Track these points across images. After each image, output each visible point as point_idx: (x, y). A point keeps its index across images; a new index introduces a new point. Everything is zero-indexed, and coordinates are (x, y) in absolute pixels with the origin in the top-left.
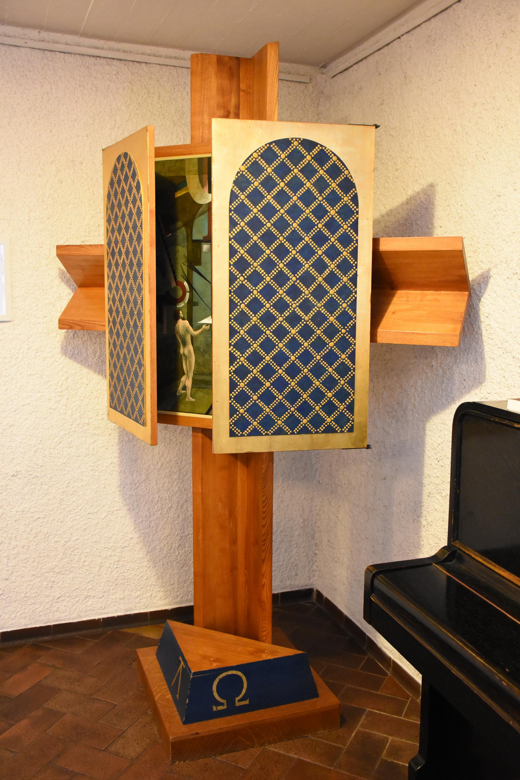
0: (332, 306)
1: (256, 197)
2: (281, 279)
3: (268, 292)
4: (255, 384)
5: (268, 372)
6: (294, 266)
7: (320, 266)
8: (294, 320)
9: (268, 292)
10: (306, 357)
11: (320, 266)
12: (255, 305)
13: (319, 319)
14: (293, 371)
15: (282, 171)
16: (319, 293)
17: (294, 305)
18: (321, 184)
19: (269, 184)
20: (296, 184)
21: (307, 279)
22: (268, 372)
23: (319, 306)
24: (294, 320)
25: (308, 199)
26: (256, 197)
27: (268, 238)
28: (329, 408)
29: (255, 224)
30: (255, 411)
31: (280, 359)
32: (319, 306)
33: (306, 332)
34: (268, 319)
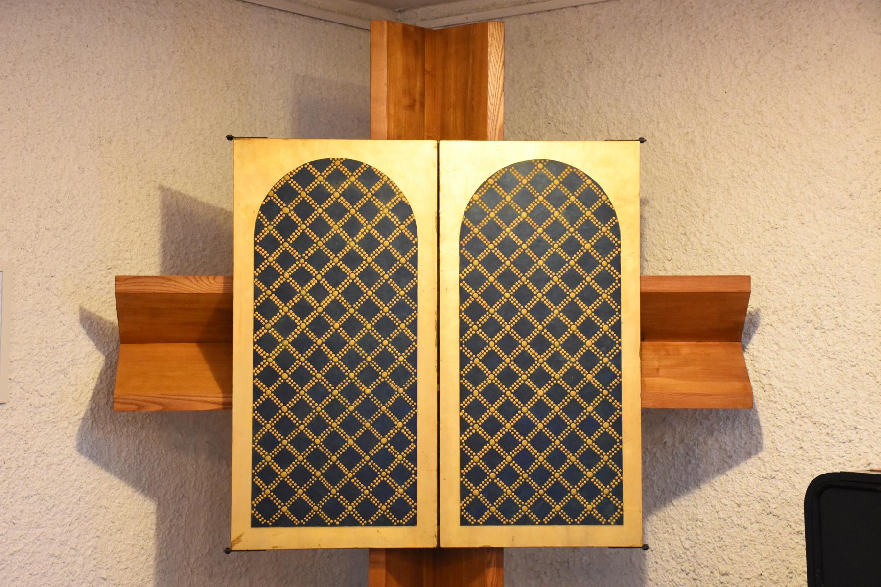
0: (589, 360)
3: (508, 344)
5: (508, 442)
7: (573, 312)
11: (573, 312)
13: (573, 377)
16: (573, 345)
17: (541, 360)
18: (573, 214)
22: (508, 442)
23: (573, 361)
28: (590, 492)
30: (492, 492)
31: (524, 426)
32: (573, 361)
33: (557, 394)
34: (508, 377)
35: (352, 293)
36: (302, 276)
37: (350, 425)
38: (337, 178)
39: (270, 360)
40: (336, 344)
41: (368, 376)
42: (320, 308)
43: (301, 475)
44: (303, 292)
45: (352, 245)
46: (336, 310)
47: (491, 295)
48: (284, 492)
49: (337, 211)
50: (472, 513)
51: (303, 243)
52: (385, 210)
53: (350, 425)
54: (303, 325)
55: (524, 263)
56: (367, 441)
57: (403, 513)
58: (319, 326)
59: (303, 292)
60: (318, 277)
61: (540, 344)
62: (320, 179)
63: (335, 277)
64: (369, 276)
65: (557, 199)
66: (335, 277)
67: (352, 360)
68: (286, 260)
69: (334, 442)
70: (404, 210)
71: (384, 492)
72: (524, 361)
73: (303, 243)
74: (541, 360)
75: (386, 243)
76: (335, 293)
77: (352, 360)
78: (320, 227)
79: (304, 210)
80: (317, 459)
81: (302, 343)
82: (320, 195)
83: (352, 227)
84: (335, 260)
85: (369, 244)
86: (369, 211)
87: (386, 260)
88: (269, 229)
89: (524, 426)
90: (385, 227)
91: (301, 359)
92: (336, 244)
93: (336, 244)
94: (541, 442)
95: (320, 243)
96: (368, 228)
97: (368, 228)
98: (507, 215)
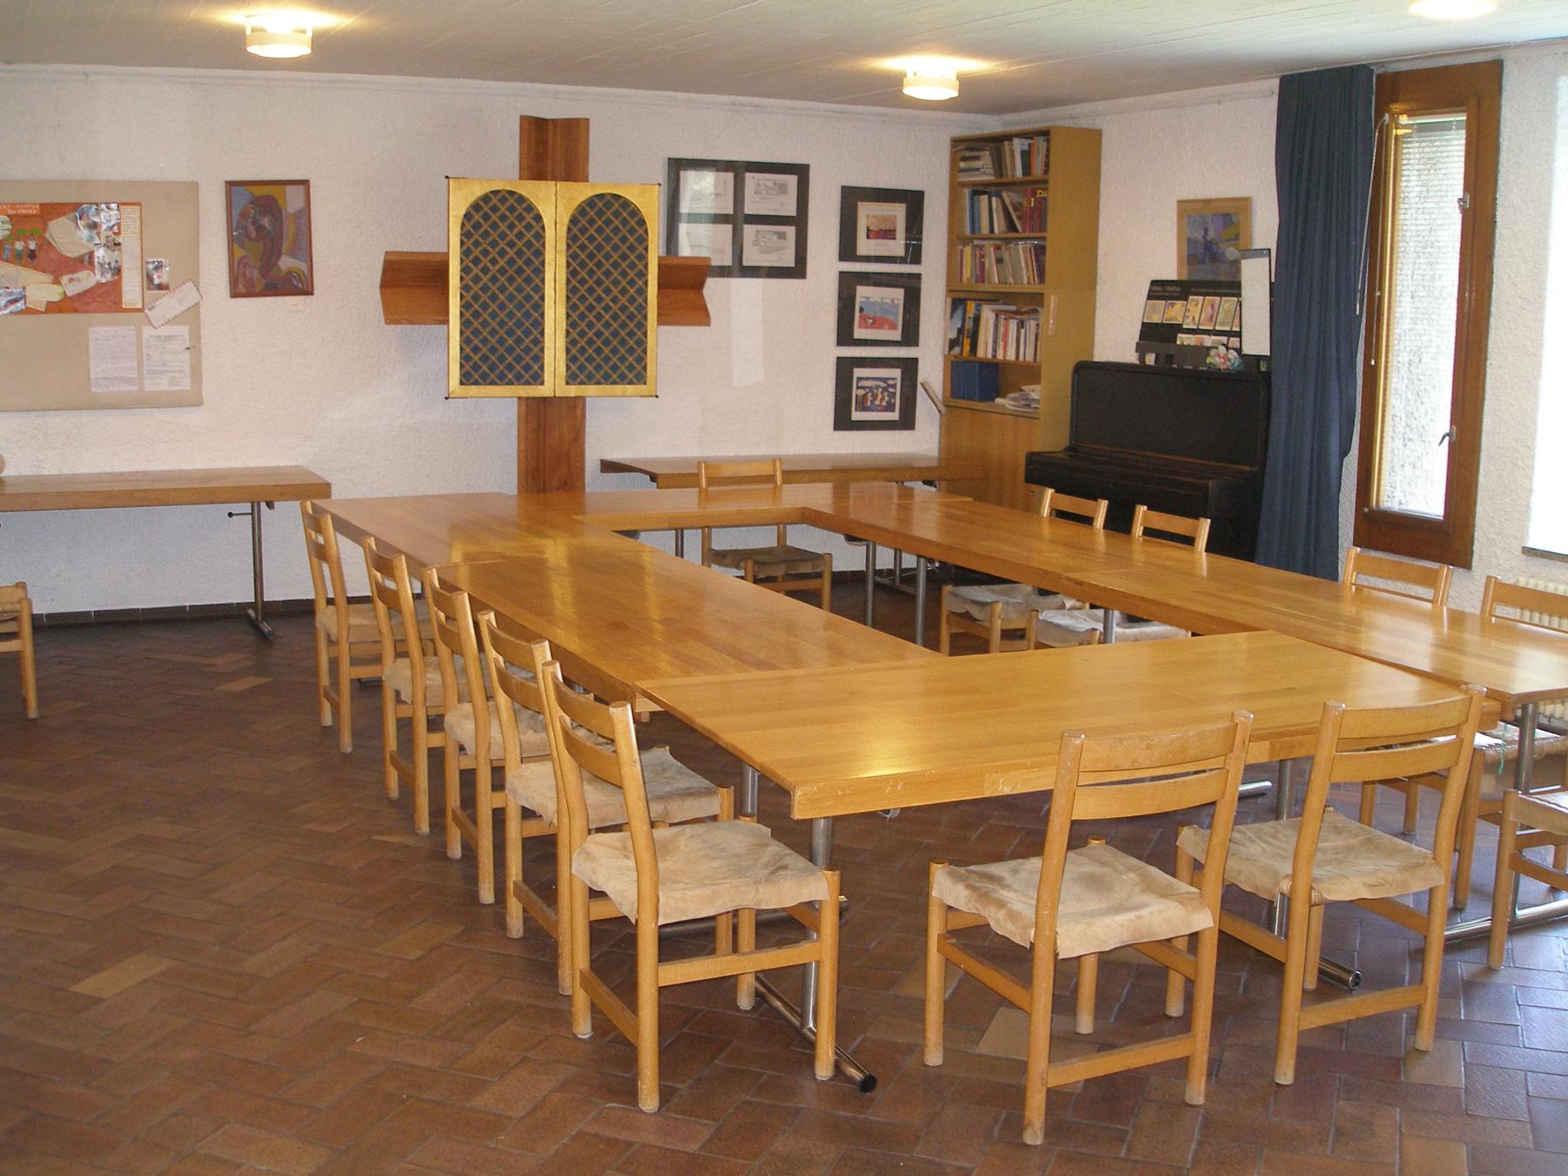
1: (583, 230)
2: (599, 282)
3: (591, 291)
4: (582, 351)
5: (590, 342)
6: (607, 274)
7: (624, 274)
8: (607, 309)
9: (591, 291)
10: (615, 334)
11: (624, 274)
12: (583, 299)
13: (623, 309)
14: (607, 343)
15: (600, 214)
18: (624, 222)
19: (592, 222)
20: (608, 222)
21: (616, 283)
22: (590, 342)
23: (623, 300)
24: (607, 309)
25: (616, 231)
26: (583, 230)
27: (591, 256)
28: (631, 368)
29: (583, 247)
30: (582, 368)
31: (599, 334)
32: (623, 300)
33: (615, 317)
34: (591, 308)
35: (511, 262)
36: (485, 253)
37: (510, 333)
38: (503, 200)
39: (468, 297)
40: (502, 289)
41: (520, 306)
42: (494, 269)
43: (485, 358)
44: (485, 261)
45: (511, 236)
46: (502, 271)
47: (583, 265)
48: (476, 367)
49: (503, 218)
50: (571, 378)
51: (486, 235)
52: (529, 218)
53: (510, 333)
54: (485, 279)
55: (599, 248)
56: (519, 341)
57: (538, 379)
58: (494, 279)
59: (485, 261)
60: (493, 253)
61: (607, 291)
62: (495, 200)
63: (502, 253)
64: (520, 253)
65: (616, 214)
66: (502, 253)
67: (511, 298)
68: (477, 244)
69: (501, 341)
70: (538, 218)
71: (527, 368)
72: (599, 299)
73: (486, 235)
74: (608, 300)
75: (529, 236)
76: (502, 263)
77: (511, 298)
78: (494, 226)
79: (486, 217)
80: (493, 350)
81: (485, 289)
82: (495, 209)
83: (511, 227)
84: (502, 244)
85: (520, 236)
86: (520, 218)
87: (529, 245)
88: (468, 227)
89: (599, 334)
90: (529, 227)
91: (484, 297)
92: (503, 236)
93: (503, 236)
94: (607, 343)
95: (494, 235)
96: (519, 227)
97: (519, 227)
98: (592, 222)
